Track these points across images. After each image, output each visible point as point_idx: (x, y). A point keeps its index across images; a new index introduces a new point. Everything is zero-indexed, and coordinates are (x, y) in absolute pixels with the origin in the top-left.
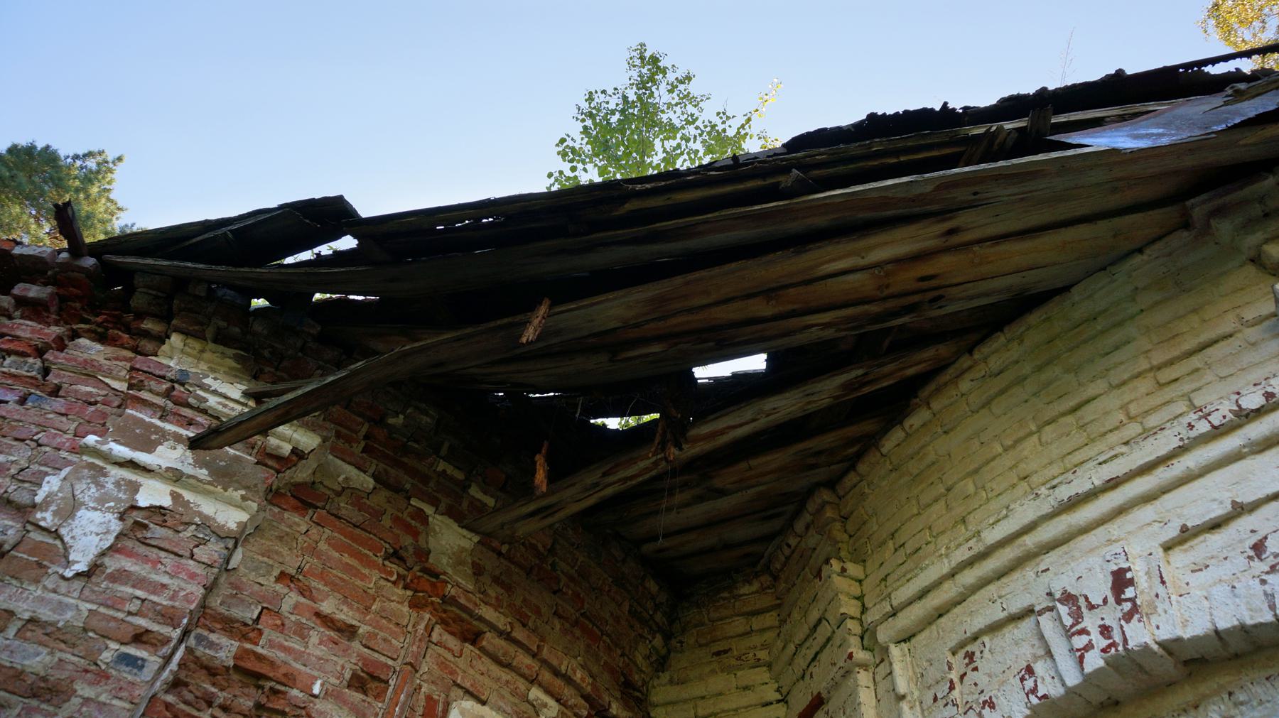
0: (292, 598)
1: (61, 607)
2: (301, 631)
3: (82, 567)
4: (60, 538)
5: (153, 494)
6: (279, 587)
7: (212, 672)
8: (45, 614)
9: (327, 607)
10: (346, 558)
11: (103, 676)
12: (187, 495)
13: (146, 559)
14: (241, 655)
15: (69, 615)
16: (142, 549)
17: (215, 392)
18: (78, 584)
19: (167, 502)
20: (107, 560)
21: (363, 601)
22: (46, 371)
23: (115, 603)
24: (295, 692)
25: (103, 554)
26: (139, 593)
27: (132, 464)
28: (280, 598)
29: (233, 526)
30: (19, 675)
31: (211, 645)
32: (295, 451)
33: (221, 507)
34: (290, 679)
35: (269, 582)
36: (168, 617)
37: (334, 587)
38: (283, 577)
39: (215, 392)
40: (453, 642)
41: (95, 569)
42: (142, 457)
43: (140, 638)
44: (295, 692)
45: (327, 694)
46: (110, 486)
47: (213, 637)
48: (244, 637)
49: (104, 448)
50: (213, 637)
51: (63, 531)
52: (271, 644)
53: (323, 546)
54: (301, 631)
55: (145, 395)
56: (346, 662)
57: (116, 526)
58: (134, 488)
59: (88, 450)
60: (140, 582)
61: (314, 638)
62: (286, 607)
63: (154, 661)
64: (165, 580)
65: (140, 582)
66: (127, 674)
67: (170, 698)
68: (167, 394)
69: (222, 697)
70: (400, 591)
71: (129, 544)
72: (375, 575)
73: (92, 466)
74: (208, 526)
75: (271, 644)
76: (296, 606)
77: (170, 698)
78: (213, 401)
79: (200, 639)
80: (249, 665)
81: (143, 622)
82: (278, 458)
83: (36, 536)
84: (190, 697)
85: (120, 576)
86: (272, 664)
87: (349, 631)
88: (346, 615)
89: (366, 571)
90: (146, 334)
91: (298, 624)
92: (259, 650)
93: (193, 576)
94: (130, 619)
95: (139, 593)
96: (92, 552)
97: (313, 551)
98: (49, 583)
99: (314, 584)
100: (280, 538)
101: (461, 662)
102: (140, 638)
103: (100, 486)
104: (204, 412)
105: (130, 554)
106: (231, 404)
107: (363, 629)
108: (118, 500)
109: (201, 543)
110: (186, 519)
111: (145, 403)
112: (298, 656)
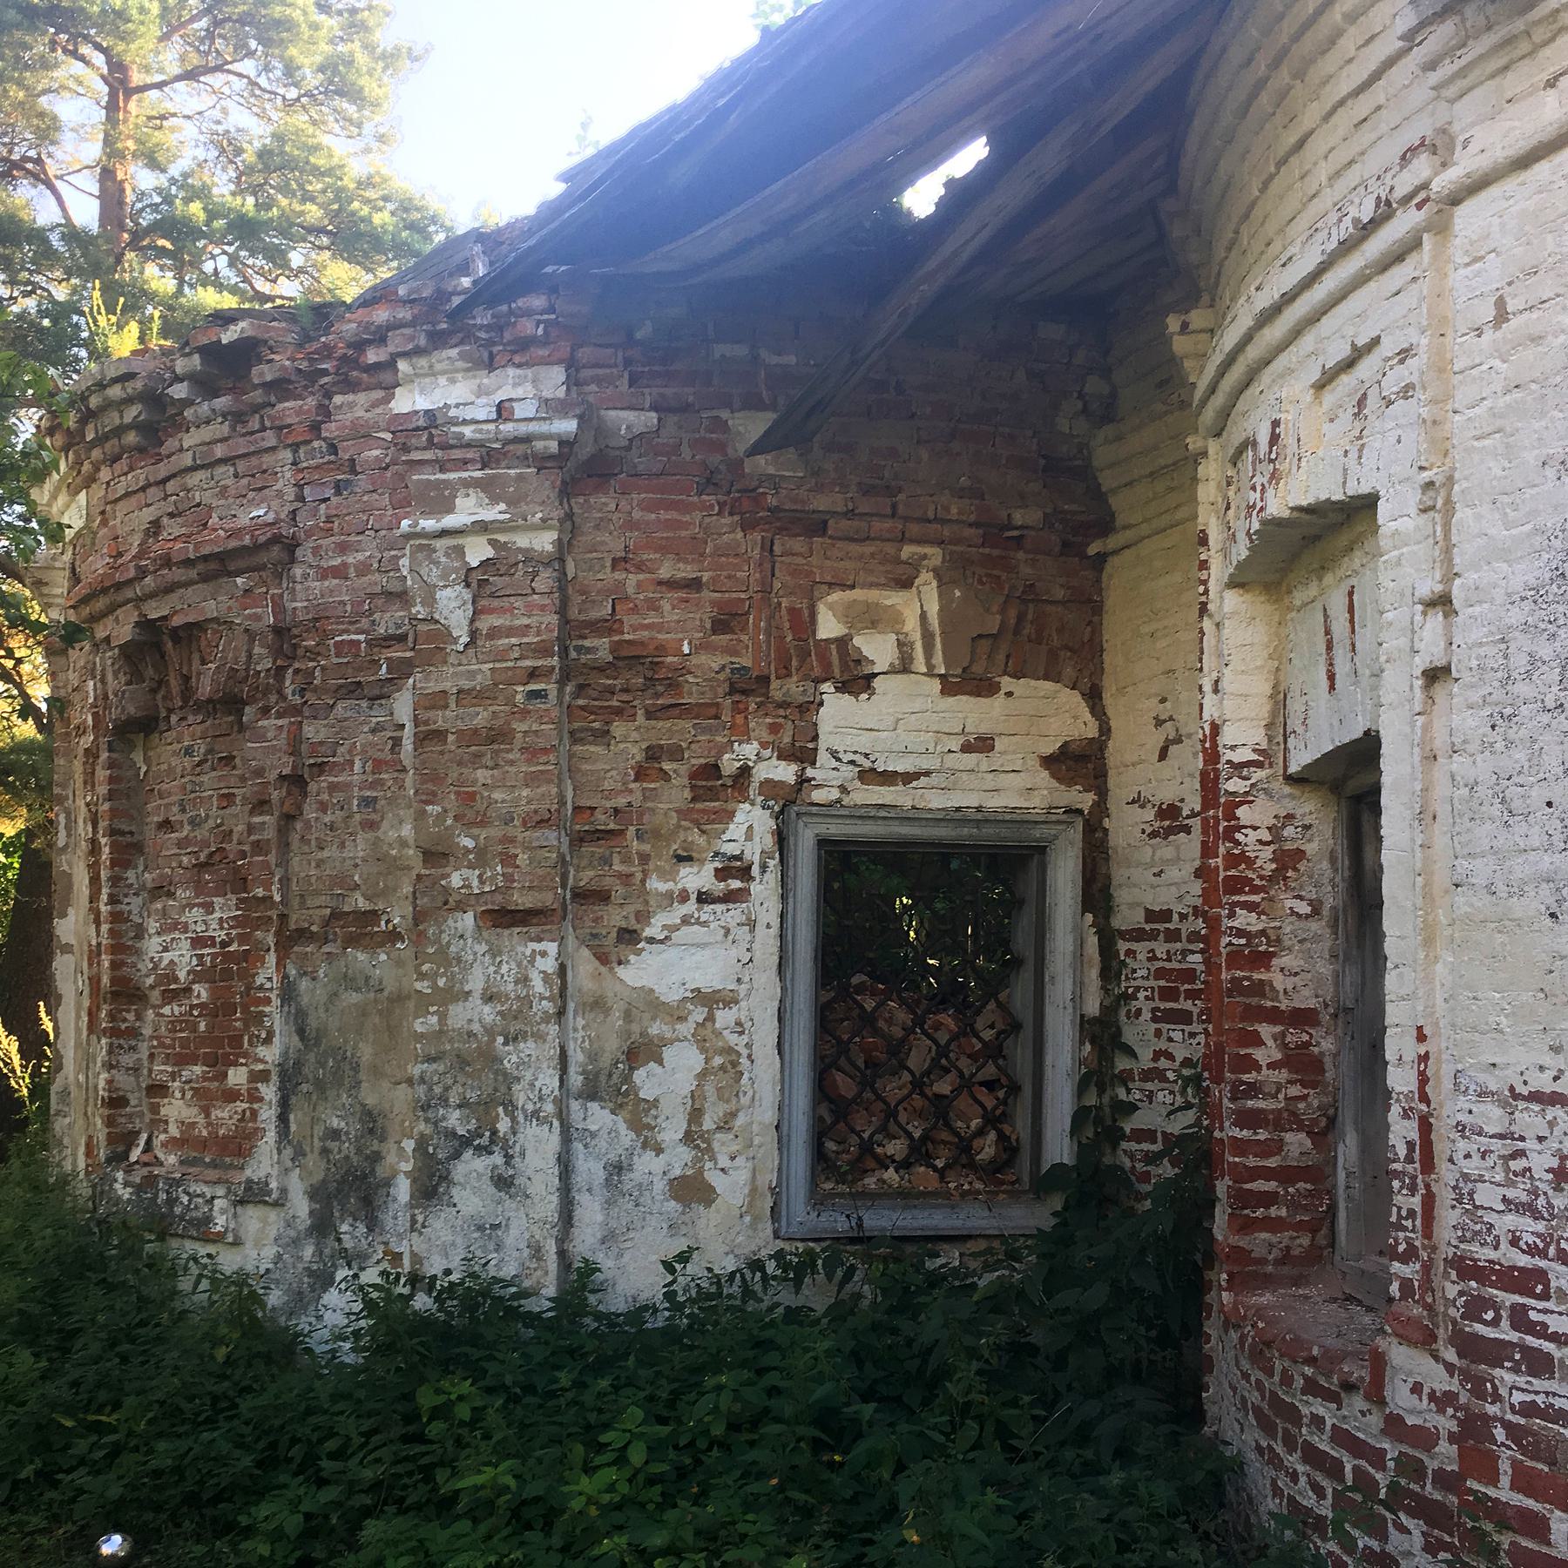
0: (632, 579)
1: (472, 675)
2: (653, 606)
3: (465, 639)
4: (437, 622)
5: (478, 552)
6: (619, 575)
7: (601, 669)
8: (466, 684)
9: (665, 572)
10: (664, 515)
11: (525, 713)
12: (502, 538)
13: (502, 611)
14: (615, 648)
15: (479, 677)
16: (496, 603)
17: (465, 422)
18: (471, 651)
19: (489, 553)
20: (478, 624)
21: (693, 548)
22: (333, 449)
23: (501, 656)
24: (670, 659)
25: (472, 621)
26: (514, 640)
27: (444, 533)
28: (621, 584)
29: (549, 548)
30: (476, 731)
31: (589, 650)
32: (561, 443)
33: (531, 535)
34: (661, 649)
35: (608, 576)
36: (543, 650)
37: (663, 549)
38: (616, 563)
39: (465, 422)
40: (798, 544)
41: (474, 634)
42: (450, 521)
43: (533, 674)
44: (670, 659)
45: (697, 649)
46: (443, 559)
47: (587, 643)
48: (610, 632)
49: (418, 529)
50: (587, 643)
51: (437, 616)
52: (635, 629)
53: (637, 514)
54: (653, 606)
55: (416, 456)
56: (703, 615)
57: (467, 595)
58: (460, 551)
59: (408, 537)
60: (510, 631)
61: (667, 607)
62: (630, 590)
63: (552, 688)
64: (526, 621)
65: (510, 631)
66: (539, 705)
67: (581, 702)
68: (431, 444)
69: (618, 683)
70: (727, 520)
71: (483, 602)
72: (697, 516)
73: (421, 548)
74: (529, 557)
75: (635, 629)
76: (639, 584)
77: (581, 702)
78: (468, 431)
79: (579, 649)
80: (624, 653)
81: (528, 663)
82: (552, 457)
83: (422, 627)
84: (595, 694)
85: (494, 633)
86: (642, 643)
87: (695, 584)
88: (686, 571)
89: (687, 518)
90: (378, 366)
91: (647, 600)
92: (627, 637)
93: (543, 608)
94: (520, 664)
95: (514, 640)
96: (465, 623)
97: (631, 525)
98: (452, 659)
99: (645, 557)
100: (597, 527)
101: (814, 560)
102: (533, 674)
103: (437, 563)
104: (469, 445)
105: (491, 611)
106: (485, 427)
107: (706, 576)
108: (456, 570)
109: (535, 574)
110: (512, 560)
111: (421, 462)
112: (659, 628)
